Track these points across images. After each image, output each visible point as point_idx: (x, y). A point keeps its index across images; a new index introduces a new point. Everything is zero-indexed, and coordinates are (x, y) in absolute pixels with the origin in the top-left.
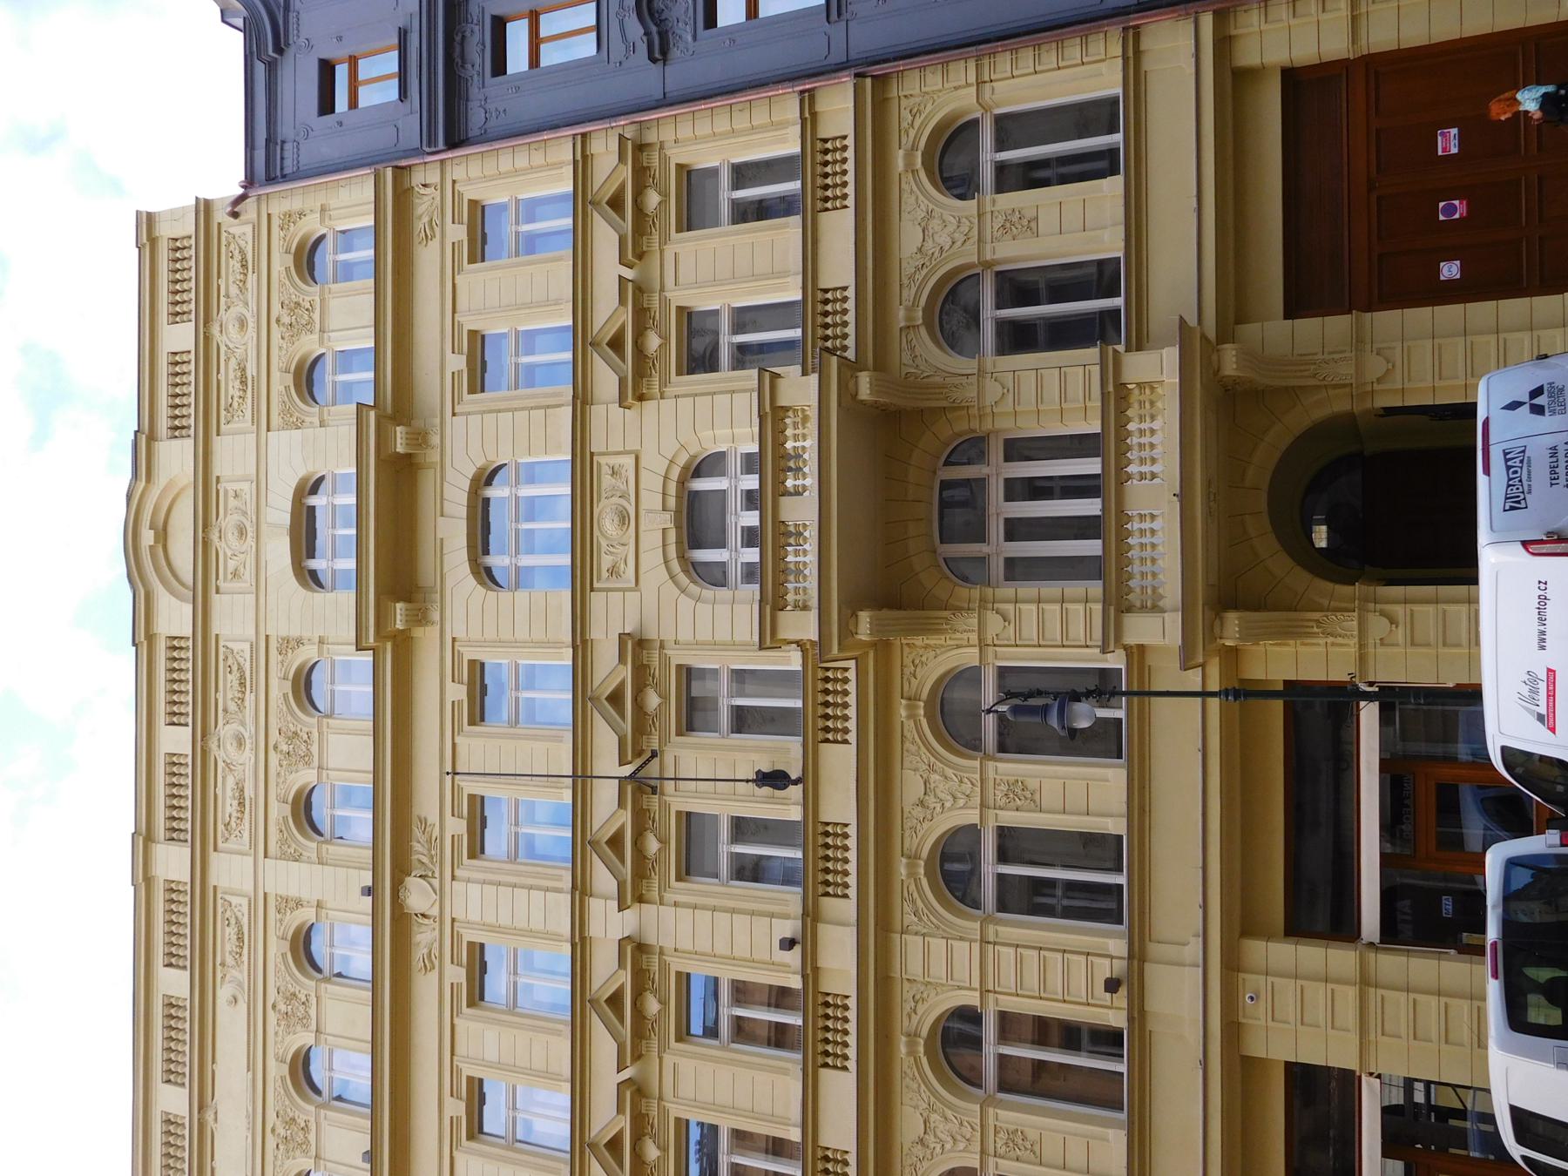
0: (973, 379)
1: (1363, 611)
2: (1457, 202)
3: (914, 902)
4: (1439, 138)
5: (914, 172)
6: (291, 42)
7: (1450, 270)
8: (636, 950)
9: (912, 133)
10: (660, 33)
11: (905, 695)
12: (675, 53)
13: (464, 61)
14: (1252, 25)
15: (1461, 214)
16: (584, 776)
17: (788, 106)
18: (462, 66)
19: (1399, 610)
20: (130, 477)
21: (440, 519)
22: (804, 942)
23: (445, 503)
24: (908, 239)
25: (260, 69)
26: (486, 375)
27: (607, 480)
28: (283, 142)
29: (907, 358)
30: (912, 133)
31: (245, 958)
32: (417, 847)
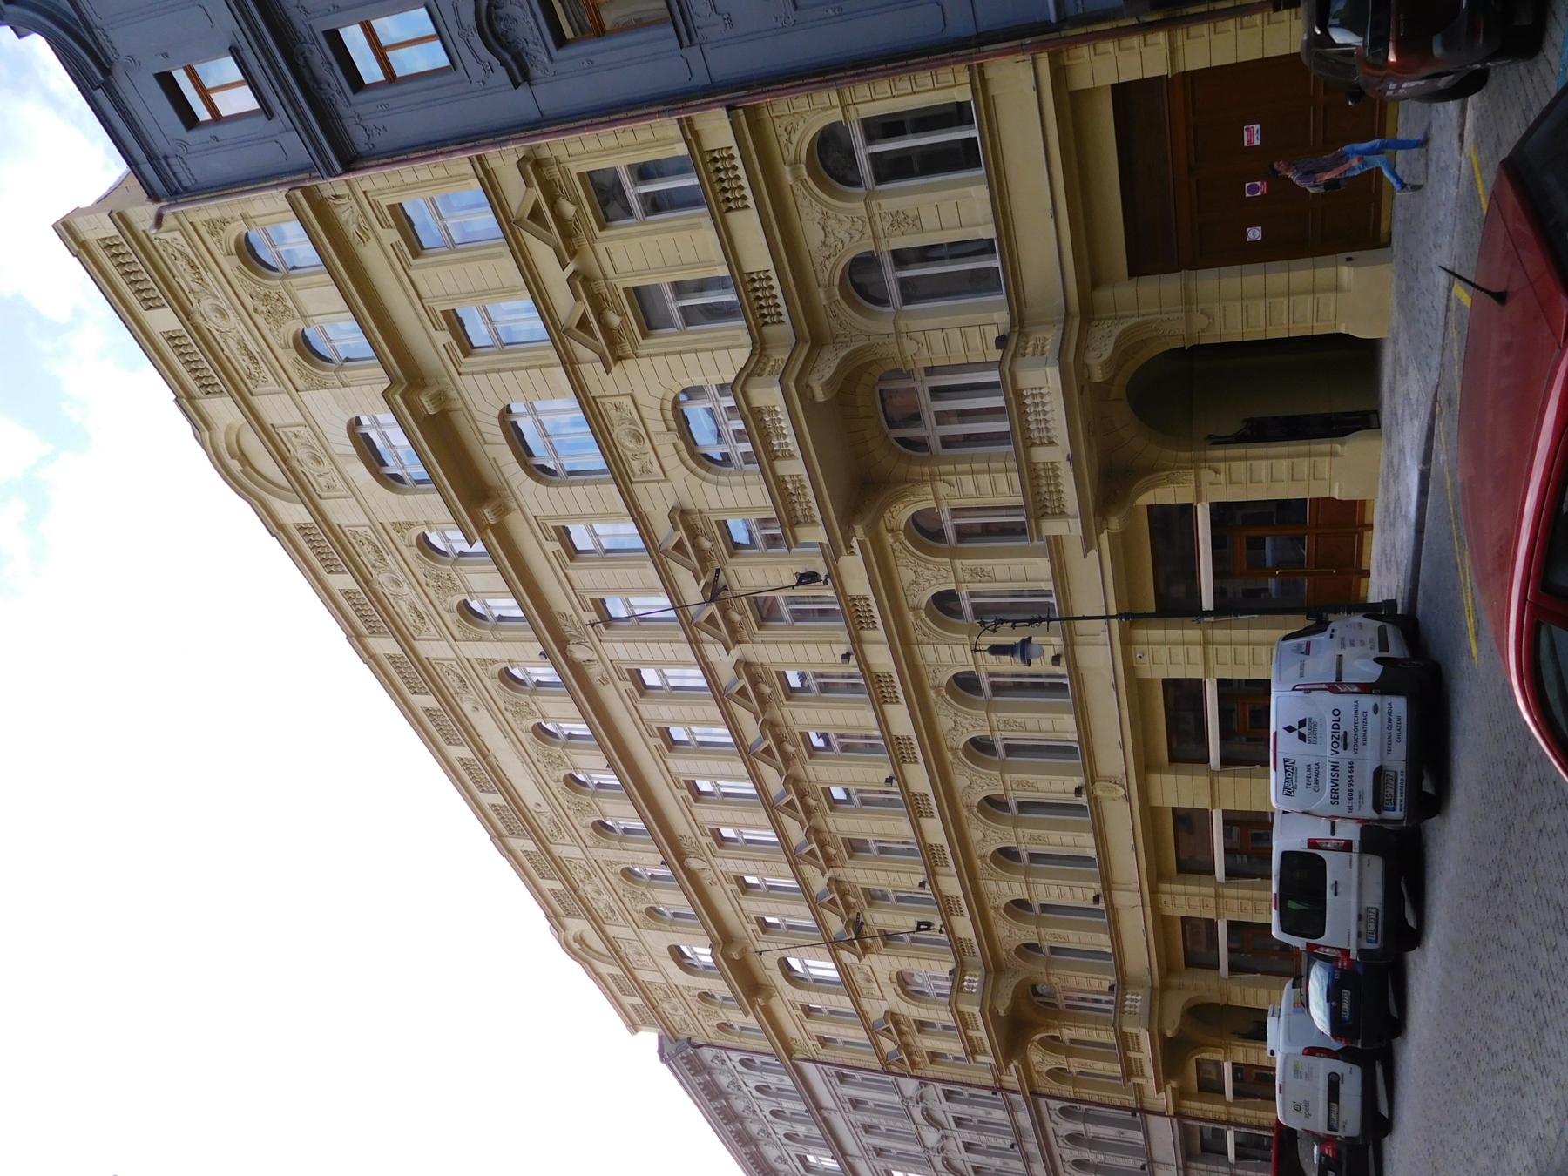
0: (892, 339)
1: (1197, 468)
2: (1259, 183)
3: (922, 629)
4: (1245, 133)
5: (803, 182)
6: (112, 59)
7: (1254, 234)
8: (745, 666)
9: (792, 148)
10: (514, 58)
11: (787, 160)
12: (535, 72)
13: (318, 83)
14: (1083, 57)
15: (1262, 192)
16: (681, 607)
17: (668, 127)
18: (321, 89)
19: (1222, 466)
20: (187, 426)
21: (486, 447)
22: (857, 649)
23: (502, 469)
24: (812, 235)
25: (100, 94)
26: (466, 328)
27: (613, 413)
28: (166, 158)
29: (834, 323)
30: (792, 148)
31: (470, 688)
32: (566, 629)
